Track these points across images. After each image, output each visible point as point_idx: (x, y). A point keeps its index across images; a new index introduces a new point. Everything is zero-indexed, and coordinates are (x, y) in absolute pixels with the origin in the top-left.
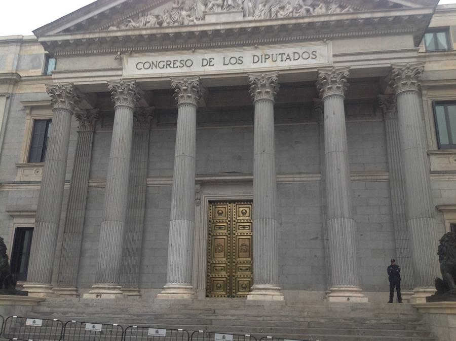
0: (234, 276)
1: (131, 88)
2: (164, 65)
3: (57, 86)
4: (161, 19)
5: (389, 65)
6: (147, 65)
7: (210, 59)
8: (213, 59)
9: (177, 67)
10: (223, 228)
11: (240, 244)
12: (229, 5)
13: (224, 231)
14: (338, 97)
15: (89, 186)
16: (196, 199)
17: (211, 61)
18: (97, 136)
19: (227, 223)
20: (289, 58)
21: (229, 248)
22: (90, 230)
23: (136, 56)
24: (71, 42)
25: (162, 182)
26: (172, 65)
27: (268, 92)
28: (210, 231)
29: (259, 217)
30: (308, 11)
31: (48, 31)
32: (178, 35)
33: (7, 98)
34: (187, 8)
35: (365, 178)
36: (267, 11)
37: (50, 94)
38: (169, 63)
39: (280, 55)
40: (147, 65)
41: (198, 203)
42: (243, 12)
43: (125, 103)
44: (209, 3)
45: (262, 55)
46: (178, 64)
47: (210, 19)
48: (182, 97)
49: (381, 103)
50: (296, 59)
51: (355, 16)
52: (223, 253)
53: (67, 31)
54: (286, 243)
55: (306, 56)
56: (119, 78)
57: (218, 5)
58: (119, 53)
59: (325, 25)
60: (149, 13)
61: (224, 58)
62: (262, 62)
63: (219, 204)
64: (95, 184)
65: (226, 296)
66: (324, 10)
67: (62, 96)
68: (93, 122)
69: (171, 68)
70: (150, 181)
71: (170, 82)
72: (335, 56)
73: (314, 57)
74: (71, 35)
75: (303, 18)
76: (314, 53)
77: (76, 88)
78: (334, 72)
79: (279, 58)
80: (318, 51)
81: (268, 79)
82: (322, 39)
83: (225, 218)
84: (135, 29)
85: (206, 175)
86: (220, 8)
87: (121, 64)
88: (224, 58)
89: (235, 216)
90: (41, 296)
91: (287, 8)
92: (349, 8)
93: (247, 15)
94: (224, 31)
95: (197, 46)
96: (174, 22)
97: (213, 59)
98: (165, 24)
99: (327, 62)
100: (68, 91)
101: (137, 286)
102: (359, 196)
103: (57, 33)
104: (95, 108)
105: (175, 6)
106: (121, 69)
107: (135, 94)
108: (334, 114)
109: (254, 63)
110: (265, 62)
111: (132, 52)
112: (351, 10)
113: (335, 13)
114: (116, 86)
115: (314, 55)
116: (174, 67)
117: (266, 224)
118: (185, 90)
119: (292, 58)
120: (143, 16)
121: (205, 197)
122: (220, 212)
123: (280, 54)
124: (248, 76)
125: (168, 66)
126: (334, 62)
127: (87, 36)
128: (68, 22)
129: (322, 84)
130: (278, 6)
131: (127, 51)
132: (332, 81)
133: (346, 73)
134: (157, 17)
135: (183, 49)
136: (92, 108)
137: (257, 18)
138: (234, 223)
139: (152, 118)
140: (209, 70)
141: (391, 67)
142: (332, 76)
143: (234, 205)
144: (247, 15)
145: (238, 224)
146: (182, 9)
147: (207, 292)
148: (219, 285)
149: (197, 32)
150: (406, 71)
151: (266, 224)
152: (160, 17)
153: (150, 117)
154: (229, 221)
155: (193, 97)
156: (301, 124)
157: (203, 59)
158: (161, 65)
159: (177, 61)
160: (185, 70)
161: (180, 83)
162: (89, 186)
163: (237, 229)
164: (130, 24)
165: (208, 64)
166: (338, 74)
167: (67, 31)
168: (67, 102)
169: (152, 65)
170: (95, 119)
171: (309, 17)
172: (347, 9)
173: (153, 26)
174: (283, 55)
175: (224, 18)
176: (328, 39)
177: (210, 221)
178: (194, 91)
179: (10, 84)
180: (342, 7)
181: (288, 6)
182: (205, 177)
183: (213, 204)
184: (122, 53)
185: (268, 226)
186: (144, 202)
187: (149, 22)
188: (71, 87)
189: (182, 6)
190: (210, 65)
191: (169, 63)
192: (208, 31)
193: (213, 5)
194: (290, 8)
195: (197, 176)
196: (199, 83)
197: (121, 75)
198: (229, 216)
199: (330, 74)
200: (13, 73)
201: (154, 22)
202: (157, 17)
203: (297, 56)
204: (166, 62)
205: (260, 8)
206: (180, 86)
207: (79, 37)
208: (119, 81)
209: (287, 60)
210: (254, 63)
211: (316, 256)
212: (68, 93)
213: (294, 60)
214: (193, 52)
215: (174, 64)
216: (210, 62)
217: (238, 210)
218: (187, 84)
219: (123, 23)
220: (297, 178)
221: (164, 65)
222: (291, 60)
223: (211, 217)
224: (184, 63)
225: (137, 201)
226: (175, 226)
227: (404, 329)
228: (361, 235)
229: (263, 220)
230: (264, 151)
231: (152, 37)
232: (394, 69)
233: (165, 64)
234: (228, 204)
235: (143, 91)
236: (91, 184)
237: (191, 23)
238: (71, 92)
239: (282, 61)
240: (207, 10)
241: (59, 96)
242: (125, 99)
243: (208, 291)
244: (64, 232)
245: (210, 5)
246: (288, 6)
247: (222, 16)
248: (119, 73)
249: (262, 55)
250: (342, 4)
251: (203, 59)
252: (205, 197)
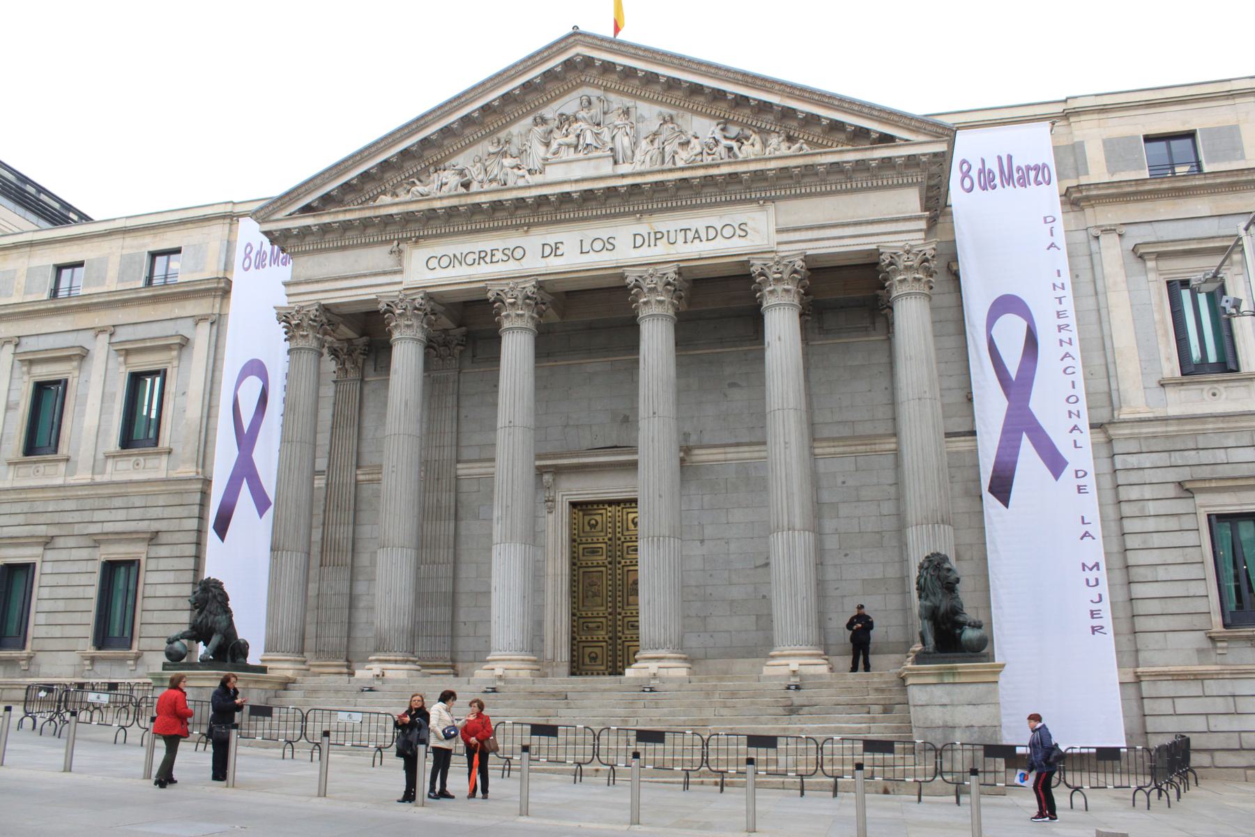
0: (620, 638)
1: (417, 306)
2: (474, 260)
3: (293, 308)
4: (471, 178)
5: (874, 247)
6: (445, 262)
7: (556, 244)
8: (562, 243)
9: (498, 262)
10: (598, 552)
11: (630, 582)
12: (587, 145)
13: (600, 558)
14: (786, 308)
15: (357, 482)
16: (546, 501)
17: (558, 248)
18: (367, 389)
19: (606, 543)
20: (699, 237)
21: (610, 588)
22: (364, 559)
23: (426, 247)
24: (314, 229)
25: (483, 471)
26: (488, 259)
27: (661, 302)
28: (574, 558)
29: (646, 536)
30: (730, 149)
31: (274, 212)
32: (497, 206)
33: (212, 324)
34: (514, 150)
35: (853, 448)
36: (656, 152)
37: (283, 324)
38: (483, 255)
39: (683, 232)
40: (445, 262)
41: (549, 508)
42: (613, 157)
43: (409, 333)
44: (552, 141)
45: (649, 233)
46: (499, 255)
47: (553, 173)
48: (507, 316)
49: (882, 305)
50: (710, 238)
52: (599, 600)
53: (307, 209)
54: (711, 575)
55: (728, 232)
58: (396, 243)
59: (759, 176)
60: (447, 164)
61: (582, 241)
62: (649, 246)
63: (595, 507)
64: (368, 477)
65: (606, 672)
66: (758, 146)
67: (302, 327)
68: (360, 361)
69: (486, 263)
70: (463, 470)
71: (485, 290)
72: (779, 231)
73: (743, 234)
74: (314, 216)
75: (718, 165)
76: (742, 227)
77: (326, 309)
78: (778, 263)
79: (681, 236)
80: (750, 223)
81: (661, 278)
82: (756, 201)
83: (602, 534)
84: (424, 197)
85: (561, 456)
86: (572, 150)
87: (400, 262)
88: (582, 241)
89: (620, 530)
90: (290, 674)
91: (691, 145)
92: (802, 144)
93: (621, 161)
94: (578, 194)
95: (532, 221)
96: (491, 181)
97: (562, 243)
98: (475, 187)
99: (766, 242)
100: (312, 317)
101: (449, 657)
102: (844, 483)
103: (290, 215)
104: (362, 336)
105: (492, 149)
106: (401, 272)
107: (426, 314)
108: (780, 339)
109: (635, 247)
110: (655, 245)
111: (419, 238)
112: (805, 146)
113: (778, 153)
114: (393, 302)
115: (743, 229)
116: (491, 262)
117: (659, 548)
118: (513, 304)
119: (703, 237)
120: (436, 171)
121: (563, 495)
122: (593, 522)
123: (681, 230)
124: (623, 273)
125: (482, 261)
126: (779, 244)
127: (341, 217)
128: (308, 192)
129: (759, 283)
130: (677, 141)
131: (410, 239)
132: (774, 279)
133: (799, 264)
134: (461, 173)
135: (507, 227)
136: (356, 336)
137: (638, 168)
138: (618, 542)
139: (462, 348)
140: (555, 264)
141: (878, 250)
142: (774, 269)
143: (618, 508)
144: (621, 161)
145: (625, 544)
146: (504, 154)
147: (572, 667)
148: (593, 655)
149: (530, 198)
150: (905, 257)
151: (659, 548)
152: (466, 171)
153: (459, 347)
154: (610, 539)
155: (527, 313)
156: (740, 349)
157: (544, 245)
158: (470, 259)
159: (497, 250)
160: (510, 267)
161: (502, 291)
162: (357, 482)
163: (625, 553)
164: (413, 189)
165: (553, 254)
166: (786, 266)
167: (307, 209)
168: (311, 336)
169: (454, 260)
170: (362, 356)
171: (729, 164)
172: (798, 145)
173: (454, 193)
174: (688, 231)
175: (578, 171)
176: (766, 200)
177: (574, 541)
178: (529, 305)
179: (215, 297)
180: (790, 139)
181: (694, 141)
182: (560, 458)
183: (579, 508)
184: (400, 241)
185: (661, 550)
186: (453, 511)
187: (446, 184)
188: (317, 310)
189: (505, 149)
190: (555, 255)
191: (483, 255)
192: (551, 195)
193: (560, 145)
194: (696, 146)
195: (539, 457)
196: (536, 290)
197: (401, 283)
198: (609, 530)
199: (772, 266)
200: (219, 279)
201: (455, 183)
202: (461, 173)
203: (712, 233)
204: (478, 254)
205: (643, 147)
206: (504, 296)
207: (326, 219)
208: (397, 293)
209: (695, 241)
210: (635, 247)
211: (764, 597)
212: (311, 320)
213: (708, 240)
214: (526, 232)
215: (493, 255)
216: (557, 248)
217: (625, 517)
218: (515, 293)
219: (402, 185)
220: (733, 454)
221: (474, 260)
222: (701, 241)
223: (576, 532)
224: (510, 254)
225: (441, 508)
226: (500, 554)
227: (869, 713)
228: (846, 555)
229: (653, 540)
230: (654, 413)
231: (452, 212)
232: (882, 254)
233: (476, 257)
234: (606, 506)
235: (442, 305)
236: (361, 477)
237: (521, 183)
238: (317, 319)
239: (685, 242)
240: (549, 156)
241: (298, 325)
242: (408, 326)
243: (575, 664)
244: (321, 565)
245: (554, 146)
246: (694, 141)
247: (574, 165)
248: (397, 278)
249: (649, 233)
250: (791, 134)
251: (544, 245)
252: (563, 495)
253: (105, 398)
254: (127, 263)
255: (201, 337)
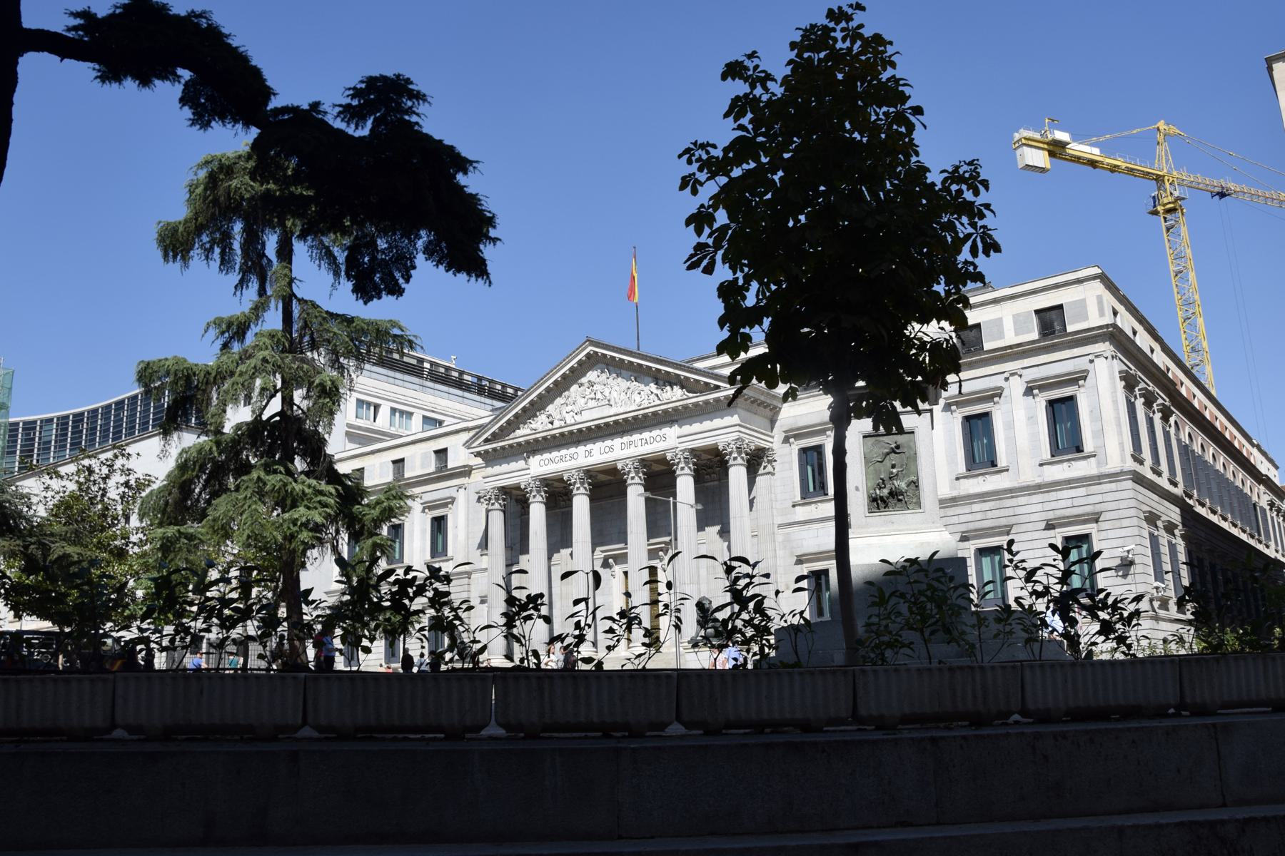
46: (568, 458)
47: (586, 416)
51: (685, 402)
53: (487, 441)
55: (658, 439)
56: (529, 476)
57: (592, 399)
84: (535, 431)
98: (557, 424)
167: (487, 441)
180: (682, 387)
207: (494, 445)
248: (527, 472)
253: (424, 531)
254: (425, 456)
255: (461, 497)
